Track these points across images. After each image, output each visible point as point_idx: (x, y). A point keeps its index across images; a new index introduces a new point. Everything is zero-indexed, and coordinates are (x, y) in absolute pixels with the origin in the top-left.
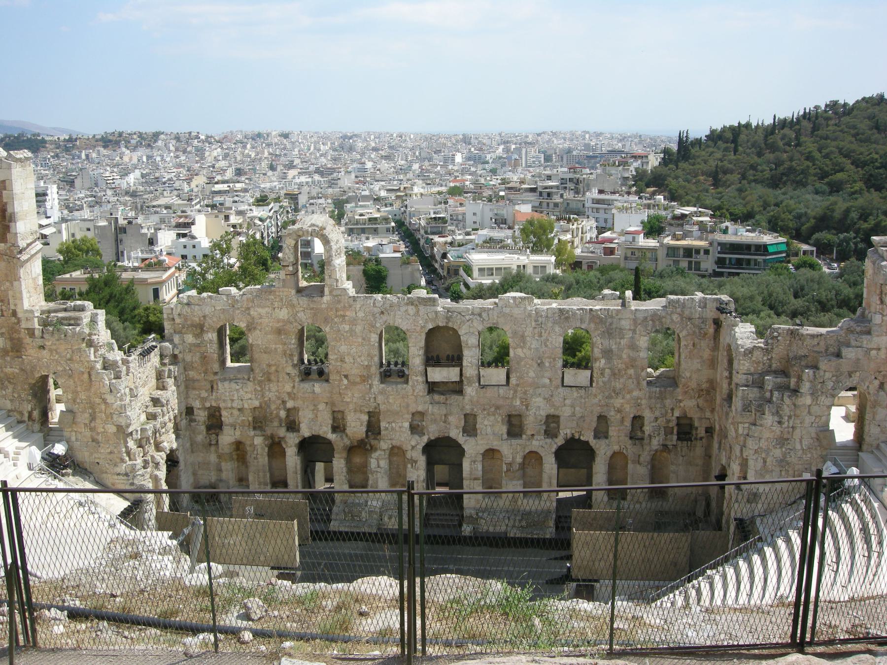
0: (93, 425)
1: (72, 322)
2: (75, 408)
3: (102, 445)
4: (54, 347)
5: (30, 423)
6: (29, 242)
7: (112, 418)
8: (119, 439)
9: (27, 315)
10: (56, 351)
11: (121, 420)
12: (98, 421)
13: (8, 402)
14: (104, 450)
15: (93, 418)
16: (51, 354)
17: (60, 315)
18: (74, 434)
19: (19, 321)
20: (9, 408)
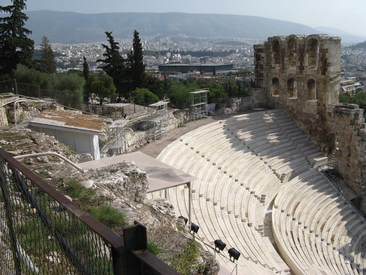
0: (348, 158)
1: (348, 112)
2: (343, 150)
3: (351, 168)
4: (338, 122)
5: (324, 152)
6: (335, 76)
7: (357, 157)
8: (359, 167)
9: (329, 107)
10: (339, 123)
11: (361, 159)
12: (351, 157)
13: (316, 142)
14: (351, 170)
15: (349, 155)
16: (337, 125)
17: (343, 109)
18: (340, 160)
19: (326, 109)
20: (317, 144)
